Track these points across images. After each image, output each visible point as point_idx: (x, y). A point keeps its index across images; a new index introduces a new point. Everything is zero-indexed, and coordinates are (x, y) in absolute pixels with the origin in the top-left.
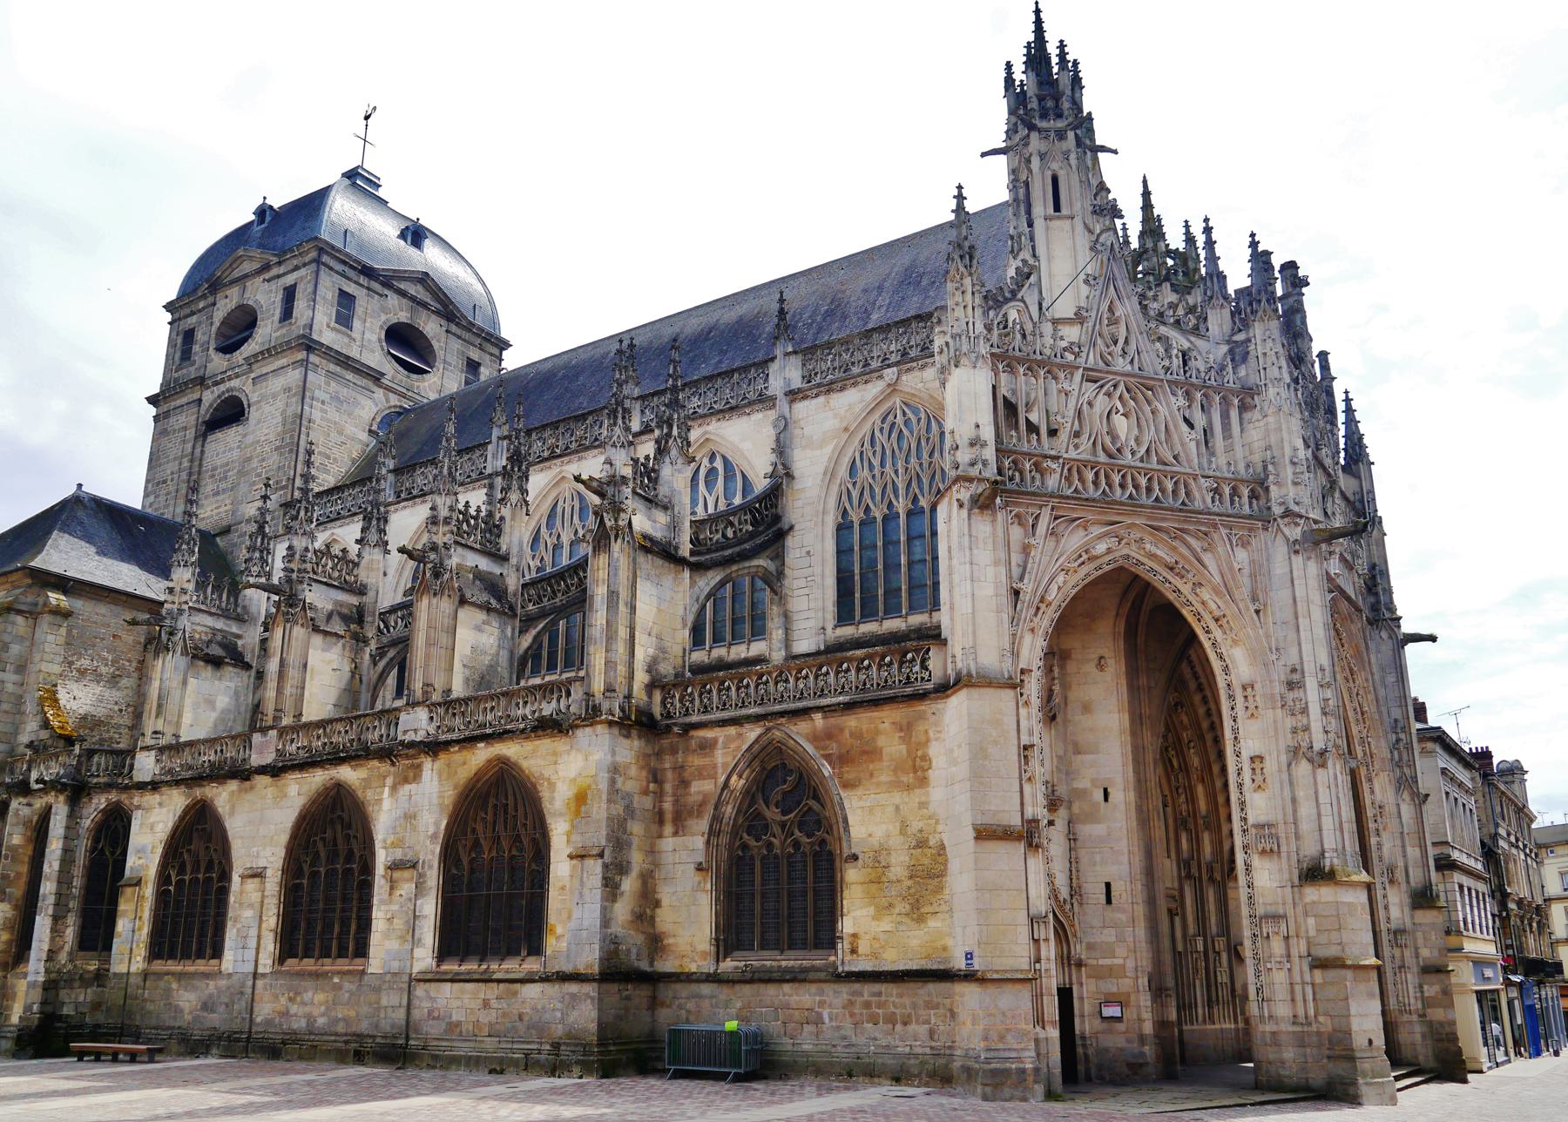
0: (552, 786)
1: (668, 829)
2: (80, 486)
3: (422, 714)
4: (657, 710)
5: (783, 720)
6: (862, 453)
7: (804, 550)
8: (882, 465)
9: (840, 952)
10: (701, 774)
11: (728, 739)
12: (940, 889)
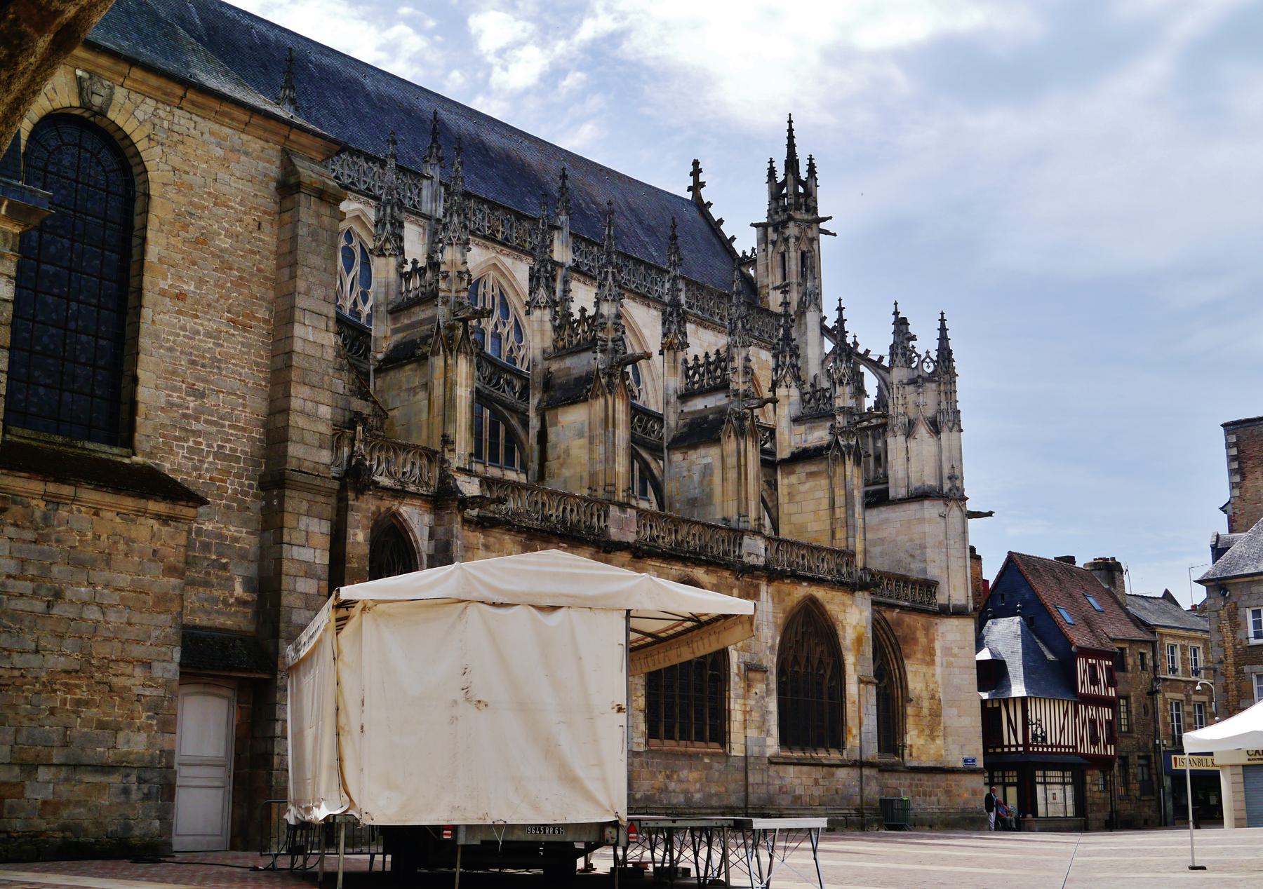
3: (760, 544)
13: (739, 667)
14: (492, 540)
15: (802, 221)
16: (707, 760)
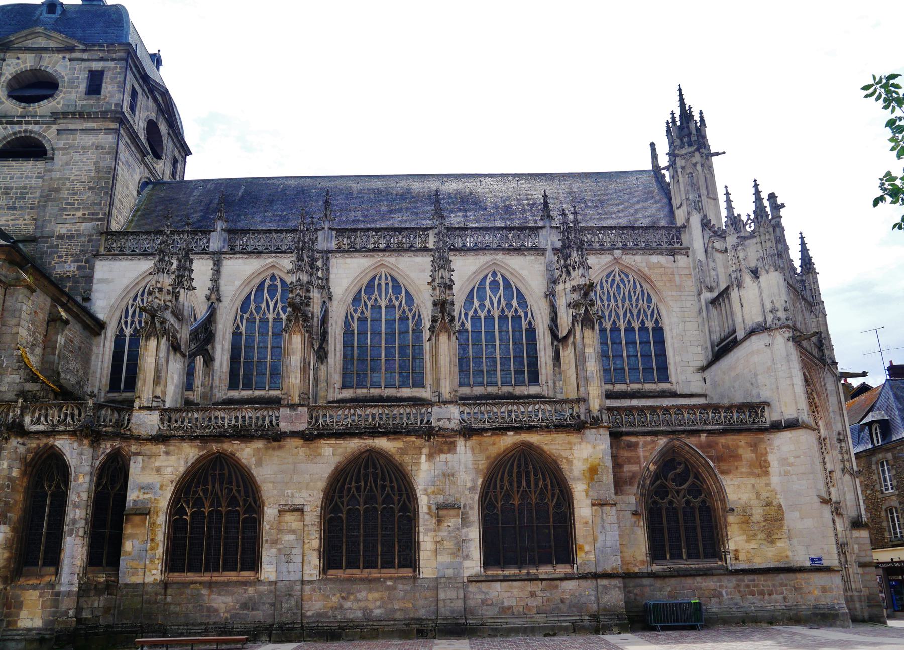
0: (570, 462)
5: (683, 435)
10: (629, 461)
11: (646, 444)
13: (430, 508)
14: (171, 448)
15: (685, 154)
16: (389, 583)
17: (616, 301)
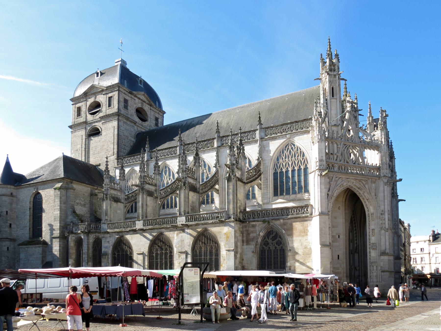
1: (245, 244)
2: (63, 153)
4: (241, 218)
6: (280, 155)
7: (266, 178)
8: (285, 158)
9: (287, 270)
10: (253, 232)
12: (310, 257)
17: (288, 158)
